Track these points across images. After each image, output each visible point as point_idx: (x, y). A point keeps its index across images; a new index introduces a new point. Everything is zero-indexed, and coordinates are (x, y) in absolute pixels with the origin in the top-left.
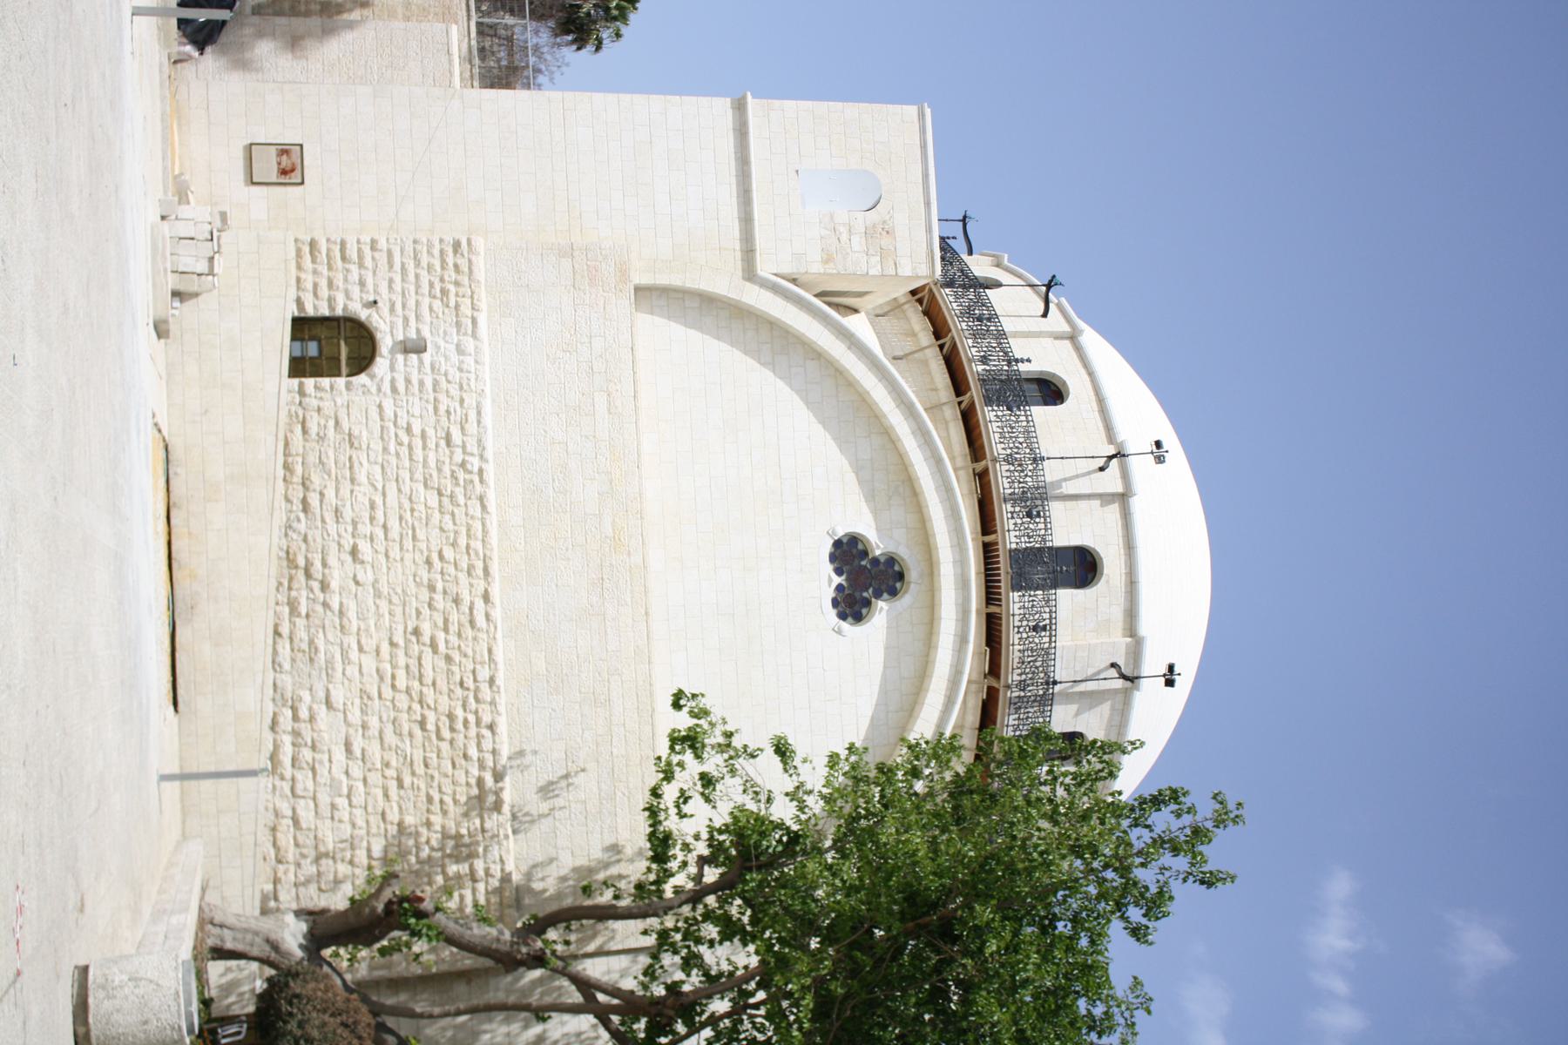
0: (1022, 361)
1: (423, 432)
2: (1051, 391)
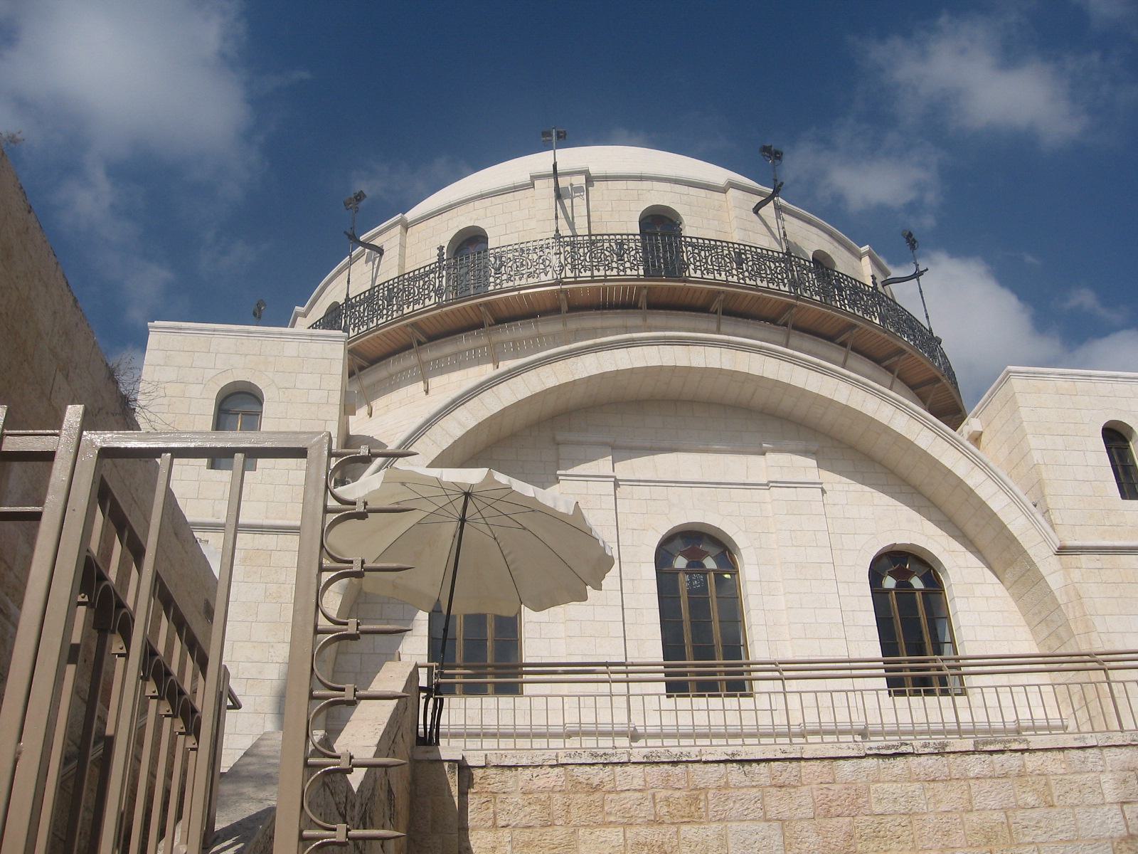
0: (440, 255)
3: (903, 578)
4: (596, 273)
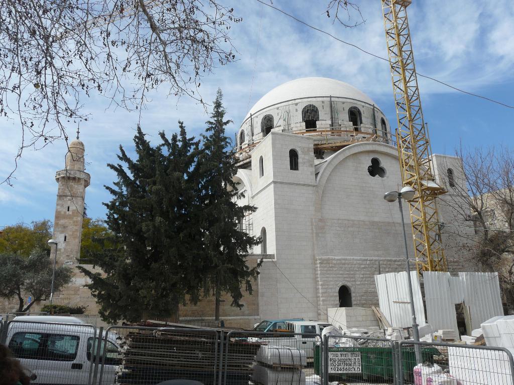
1: (363, 274)
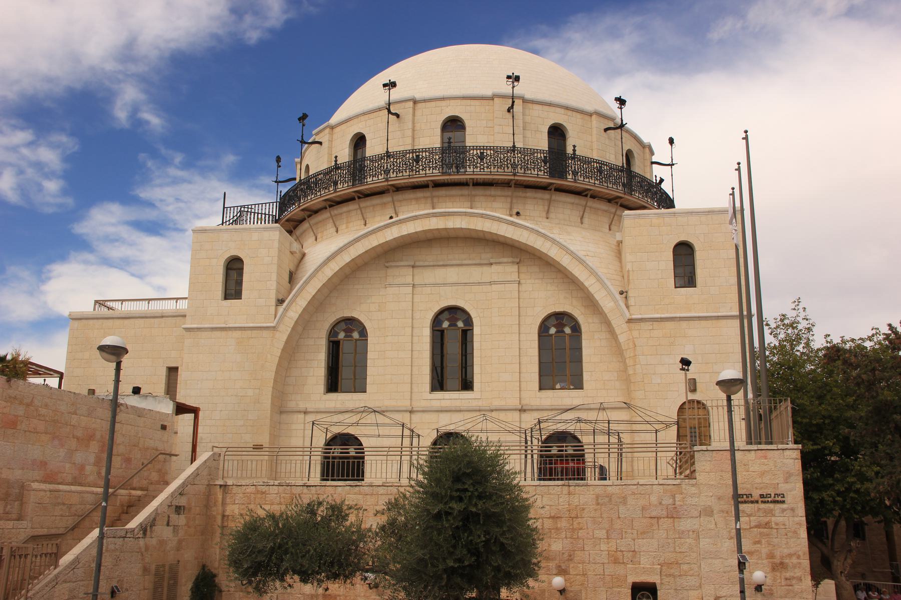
0: (336, 161)
2: (359, 141)
3: (560, 327)
4: (405, 174)
